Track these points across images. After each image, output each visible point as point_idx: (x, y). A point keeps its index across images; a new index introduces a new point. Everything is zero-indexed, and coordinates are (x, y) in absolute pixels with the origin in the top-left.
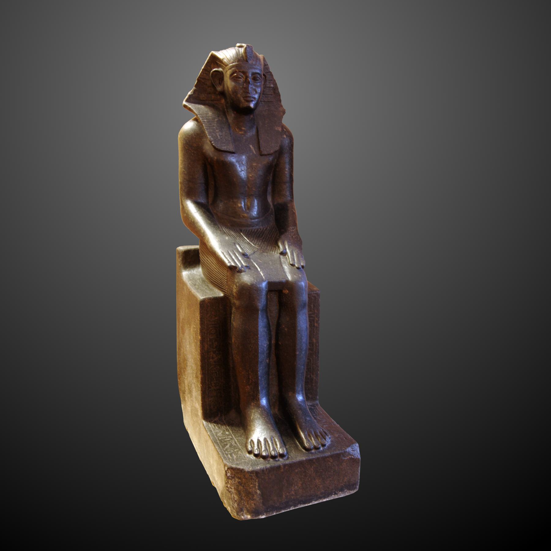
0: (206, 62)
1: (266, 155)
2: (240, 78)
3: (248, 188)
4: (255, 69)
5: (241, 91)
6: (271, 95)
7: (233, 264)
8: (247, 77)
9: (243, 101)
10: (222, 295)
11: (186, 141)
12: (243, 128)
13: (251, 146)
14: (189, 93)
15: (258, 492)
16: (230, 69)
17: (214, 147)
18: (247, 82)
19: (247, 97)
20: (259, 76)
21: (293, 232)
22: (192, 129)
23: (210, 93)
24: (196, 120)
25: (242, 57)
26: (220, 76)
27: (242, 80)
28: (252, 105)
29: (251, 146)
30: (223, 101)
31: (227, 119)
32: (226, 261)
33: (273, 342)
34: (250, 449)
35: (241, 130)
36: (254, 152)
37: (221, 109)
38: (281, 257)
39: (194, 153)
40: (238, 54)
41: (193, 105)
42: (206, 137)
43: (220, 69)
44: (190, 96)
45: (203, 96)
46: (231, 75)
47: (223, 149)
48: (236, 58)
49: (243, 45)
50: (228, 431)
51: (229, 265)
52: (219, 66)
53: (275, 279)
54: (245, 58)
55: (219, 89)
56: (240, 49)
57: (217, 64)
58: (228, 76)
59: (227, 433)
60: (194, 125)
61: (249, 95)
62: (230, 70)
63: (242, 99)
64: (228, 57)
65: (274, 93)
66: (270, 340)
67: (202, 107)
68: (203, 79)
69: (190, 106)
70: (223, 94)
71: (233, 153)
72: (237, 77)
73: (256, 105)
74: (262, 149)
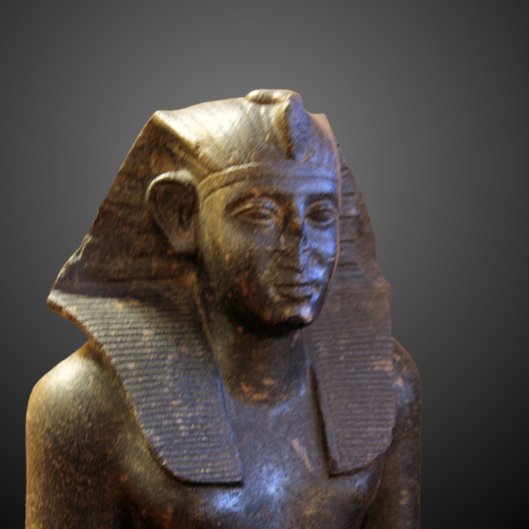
0: (130, 150)
1: (348, 474)
2: (265, 217)
4: (312, 178)
5: (270, 263)
6: (351, 241)
8: (289, 215)
9: (277, 298)
11: (55, 440)
12: (267, 382)
13: (296, 443)
14: (72, 259)
16: (227, 184)
17: (167, 472)
18: (289, 228)
19: (292, 285)
22: (78, 396)
23: (142, 254)
24: (96, 356)
25: (274, 140)
26: (182, 201)
27: (271, 224)
29: (296, 443)
30: (191, 278)
31: (208, 349)
36: (308, 464)
37: (185, 309)
39: (84, 484)
40: (254, 127)
41: (83, 300)
42: (134, 428)
43: (183, 175)
44: (72, 269)
45: (118, 265)
46: (231, 207)
47: (198, 478)
48: (251, 147)
49: (277, 94)
52: (178, 163)
54: (282, 145)
55: (180, 241)
56: (263, 109)
57: (173, 156)
58: (220, 207)
60: (86, 376)
61: (298, 278)
62: (227, 189)
63: (272, 291)
64: (218, 136)
65: (360, 233)
67: (117, 306)
68: (122, 205)
69: (72, 310)
70: (193, 258)
72: (255, 214)
74: (335, 455)
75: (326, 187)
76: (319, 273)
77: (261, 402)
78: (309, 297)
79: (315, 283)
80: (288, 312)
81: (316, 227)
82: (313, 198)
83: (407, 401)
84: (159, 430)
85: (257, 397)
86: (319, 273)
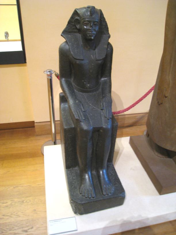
3: (89, 75)
7: (78, 118)
10: (73, 126)
15: (83, 209)
20: (97, 23)
21: (108, 96)
28: (92, 38)
32: (75, 116)
33: (95, 148)
34: (81, 192)
35: (87, 48)
38: (101, 111)
50: (75, 177)
51: (76, 118)
53: (96, 126)
56: (88, 9)
59: (74, 178)
66: (93, 149)
71: (83, 60)
73: (95, 38)
75: (97, 20)
76: (95, 33)
77: (88, 50)
78: (93, 36)
79: (94, 34)
80: (90, 38)
81: (95, 26)
82: (94, 22)
83: (110, 52)
84: (73, 52)
85: (87, 49)
86: (95, 33)
